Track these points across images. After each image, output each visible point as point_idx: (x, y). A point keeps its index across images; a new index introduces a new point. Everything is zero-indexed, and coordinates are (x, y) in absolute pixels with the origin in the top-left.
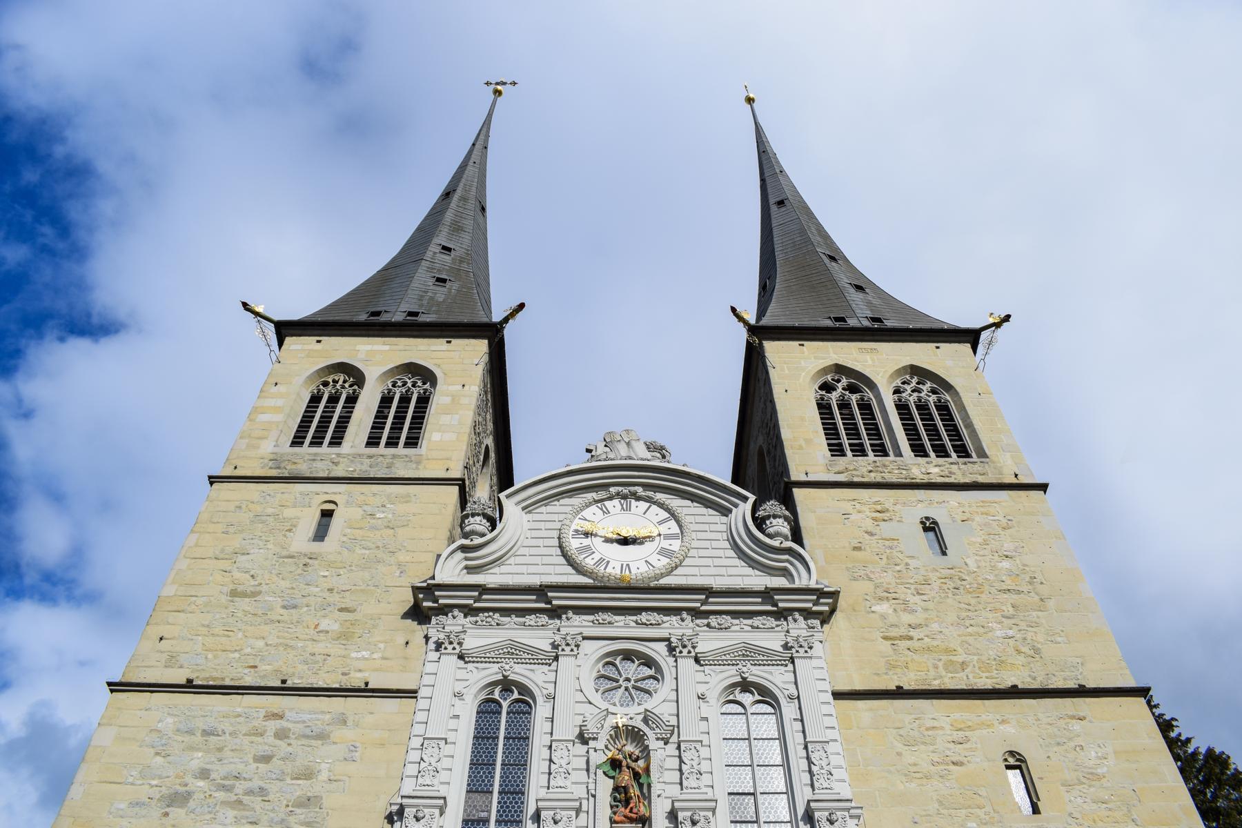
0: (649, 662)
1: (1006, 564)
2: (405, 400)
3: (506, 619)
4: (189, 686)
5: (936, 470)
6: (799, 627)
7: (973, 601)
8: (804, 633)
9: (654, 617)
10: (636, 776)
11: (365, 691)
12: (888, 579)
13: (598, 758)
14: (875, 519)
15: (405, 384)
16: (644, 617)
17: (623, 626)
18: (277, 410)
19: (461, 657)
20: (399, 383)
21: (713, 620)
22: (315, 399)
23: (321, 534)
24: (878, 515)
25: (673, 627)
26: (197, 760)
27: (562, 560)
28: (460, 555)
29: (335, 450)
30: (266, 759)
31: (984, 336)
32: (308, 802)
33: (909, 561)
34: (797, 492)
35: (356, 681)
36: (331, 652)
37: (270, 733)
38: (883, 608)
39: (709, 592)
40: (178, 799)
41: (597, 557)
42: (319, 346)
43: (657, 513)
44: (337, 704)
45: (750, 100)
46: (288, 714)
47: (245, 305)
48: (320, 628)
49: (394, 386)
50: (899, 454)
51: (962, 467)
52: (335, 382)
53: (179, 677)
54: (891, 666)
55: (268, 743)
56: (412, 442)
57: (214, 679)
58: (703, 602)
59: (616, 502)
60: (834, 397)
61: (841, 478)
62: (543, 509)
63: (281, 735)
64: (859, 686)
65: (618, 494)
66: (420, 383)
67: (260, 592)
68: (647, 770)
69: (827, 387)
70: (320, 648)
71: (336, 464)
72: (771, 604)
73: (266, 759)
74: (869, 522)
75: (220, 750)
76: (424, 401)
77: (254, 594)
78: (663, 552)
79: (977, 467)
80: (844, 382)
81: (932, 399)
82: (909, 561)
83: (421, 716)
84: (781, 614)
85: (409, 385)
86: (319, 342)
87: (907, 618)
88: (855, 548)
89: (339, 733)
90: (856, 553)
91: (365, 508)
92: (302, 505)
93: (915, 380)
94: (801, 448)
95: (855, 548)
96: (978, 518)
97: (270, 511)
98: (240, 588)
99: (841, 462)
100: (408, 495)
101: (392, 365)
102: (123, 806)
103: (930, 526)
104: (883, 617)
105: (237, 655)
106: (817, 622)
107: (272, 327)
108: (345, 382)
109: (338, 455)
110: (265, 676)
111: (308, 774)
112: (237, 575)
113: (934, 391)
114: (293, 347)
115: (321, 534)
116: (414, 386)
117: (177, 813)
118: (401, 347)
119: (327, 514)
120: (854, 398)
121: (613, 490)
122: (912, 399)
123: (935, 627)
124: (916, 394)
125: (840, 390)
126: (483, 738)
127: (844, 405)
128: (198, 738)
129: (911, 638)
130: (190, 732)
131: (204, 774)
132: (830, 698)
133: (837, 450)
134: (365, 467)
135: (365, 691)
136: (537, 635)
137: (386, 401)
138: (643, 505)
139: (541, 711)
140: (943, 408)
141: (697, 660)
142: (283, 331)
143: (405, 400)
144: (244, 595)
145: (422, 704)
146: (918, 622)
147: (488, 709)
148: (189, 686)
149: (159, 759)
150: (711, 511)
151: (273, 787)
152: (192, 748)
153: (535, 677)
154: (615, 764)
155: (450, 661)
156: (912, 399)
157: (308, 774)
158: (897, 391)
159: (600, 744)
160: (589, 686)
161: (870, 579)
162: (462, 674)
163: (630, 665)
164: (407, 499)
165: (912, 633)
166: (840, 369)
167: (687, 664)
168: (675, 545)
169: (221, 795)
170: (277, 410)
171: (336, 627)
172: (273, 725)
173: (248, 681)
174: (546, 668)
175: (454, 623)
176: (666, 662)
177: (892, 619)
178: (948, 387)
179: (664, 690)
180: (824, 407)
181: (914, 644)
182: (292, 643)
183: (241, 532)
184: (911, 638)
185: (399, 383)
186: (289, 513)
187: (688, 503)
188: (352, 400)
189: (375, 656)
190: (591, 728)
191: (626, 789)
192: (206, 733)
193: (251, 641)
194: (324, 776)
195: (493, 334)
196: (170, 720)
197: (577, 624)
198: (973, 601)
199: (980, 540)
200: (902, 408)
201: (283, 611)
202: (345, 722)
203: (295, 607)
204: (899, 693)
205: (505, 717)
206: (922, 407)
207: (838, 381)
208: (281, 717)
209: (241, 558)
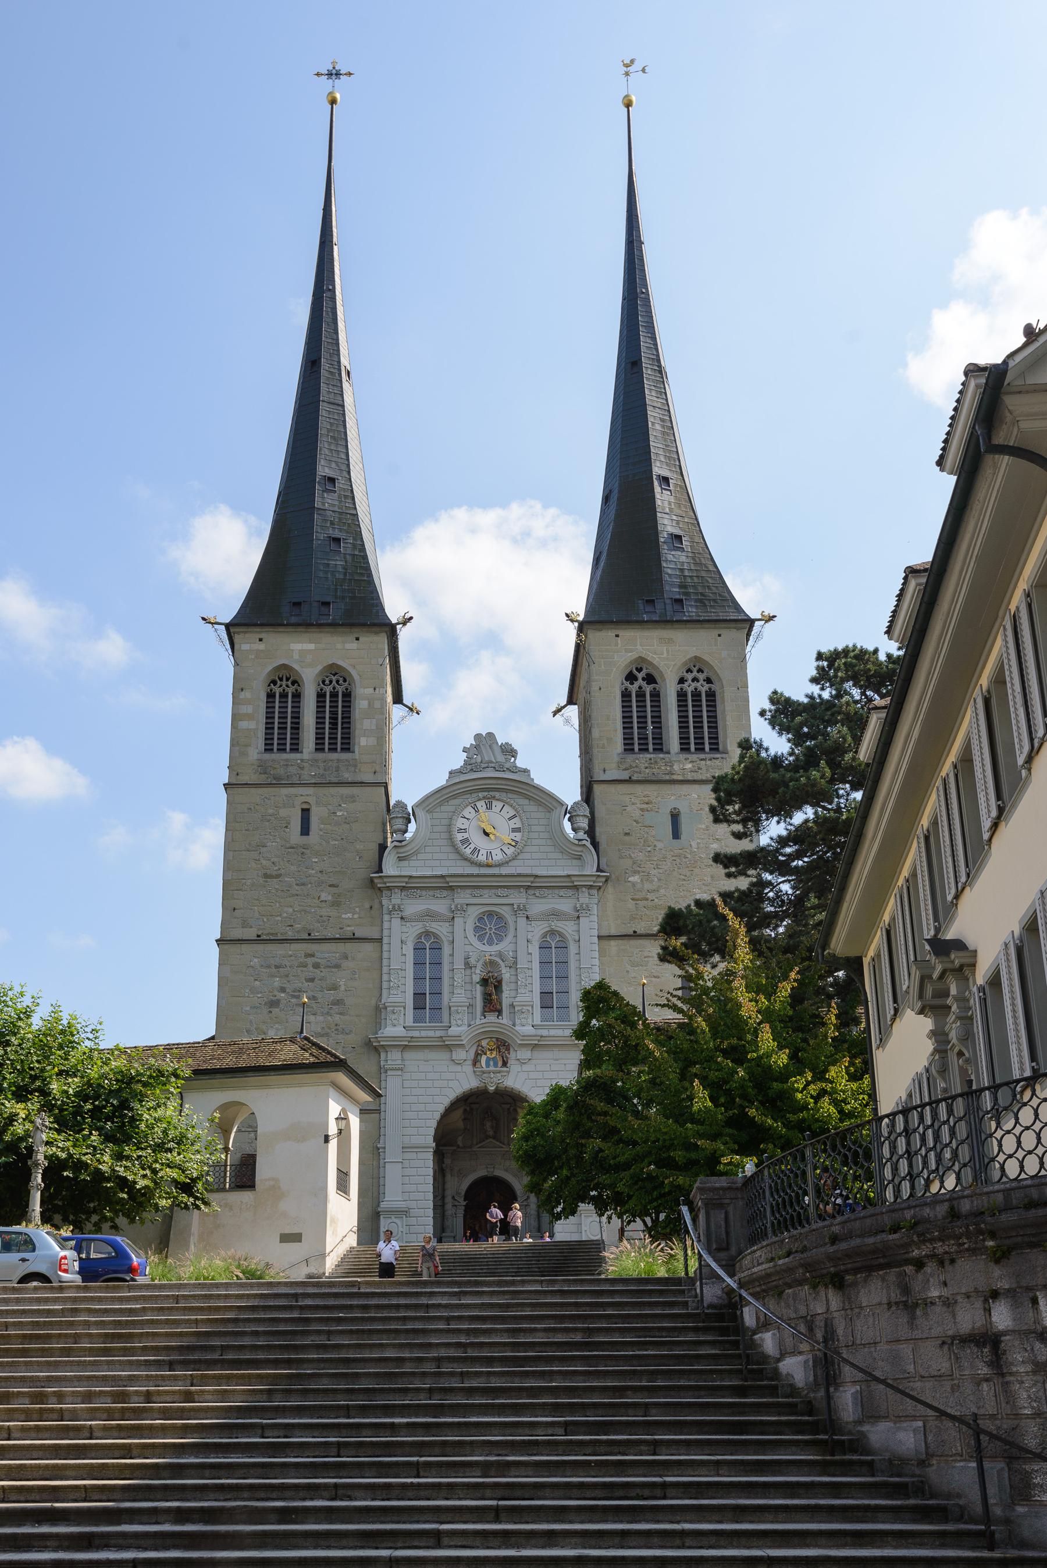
0: (500, 917)
2: (334, 695)
3: (424, 893)
4: (259, 940)
6: (584, 898)
7: (688, 874)
8: (587, 900)
9: (505, 892)
10: (496, 987)
11: (353, 938)
12: (640, 856)
13: (477, 978)
14: (642, 810)
15: (331, 682)
16: (499, 892)
17: (488, 898)
18: (249, 717)
19: (402, 918)
20: (327, 682)
21: (537, 893)
22: (270, 696)
23: (305, 830)
24: (645, 806)
25: (517, 898)
26: (277, 982)
27: (450, 849)
28: (394, 852)
29: (298, 756)
30: (312, 980)
31: (757, 623)
32: (338, 1002)
33: (656, 843)
34: (597, 789)
35: (348, 930)
36: (331, 914)
37: (310, 966)
38: (635, 879)
39: (537, 876)
40: (274, 1004)
41: (472, 846)
42: (261, 646)
43: (509, 811)
44: (341, 947)
45: (628, 105)
46: (317, 954)
47: (204, 619)
48: (322, 898)
49: (323, 682)
50: (668, 753)
51: (708, 762)
52: (281, 679)
53: (251, 933)
54: (633, 918)
55: (310, 971)
56: (347, 748)
57: (272, 934)
58: (532, 885)
59: (482, 803)
60: (634, 688)
61: (625, 776)
62: (438, 810)
63: (316, 966)
64: (613, 932)
67: (280, 875)
68: (500, 982)
69: (631, 677)
70: (324, 912)
71: (302, 768)
72: (571, 885)
73: (312, 980)
74: (638, 812)
75: (287, 976)
76: (348, 695)
77: (278, 876)
79: (717, 762)
80: (644, 671)
81: (703, 688)
82: (656, 843)
83: (385, 955)
84: (576, 888)
85: (334, 682)
86: (261, 640)
87: (647, 886)
88: (627, 834)
89: (345, 964)
90: (627, 838)
91: (330, 807)
92: (286, 804)
93: (695, 670)
94: (603, 747)
95: (627, 834)
97: (270, 811)
98: (268, 872)
99: (630, 758)
100: (353, 796)
101: (320, 668)
102: (248, 1009)
103: (675, 817)
104: (634, 884)
105: (279, 918)
106: (594, 892)
107: (223, 627)
108: (288, 679)
109: (302, 760)
110: (298, 932)
111: (335, 987)
112: (264, 862)
113: (709, 681)
114: (245, 647)
115: (305, 830)
116: (337, 682)
117: (276, 1011)
119: (306, 813)
120: (648, 689)
121: (481, 795)
122: (689, 690)
123: (662, 891)
125: (640, 681)
126: (418, 964)
127: (641, 695)
128: (274, 970)
129: (647, 899)
130: (269, 967)
131: (283, 990)
132: (596, 940)
133: (628, 748)
134: (321, 771)
135: (353, 938)
136: (440, 905)
137: (321, 696)
138: (500, 805)
139: (446, 950)
140: (711, 695)
141: (527, 918)
142: (232, 630)
144: (271, 877)
145: (385, 947)
146: (654, 888)
147: (418, 949)
148: (259, 940)
149: (257, 983)
150: (541, 809)
151: (319, 995)
152: (272, 976)
153: (441, 929)
154: (485, 982)
155: (396, 922)
156: (689, 690)
157: (335, 987)
158: (682, 681)
159: (478, 971)
160: (470, 933)
161: (631, 857)
162: (405, 929)
163: (491, 924)
164: (353, 798)
165: (650, 896)
166: (640, 664)
167: (522, 921)
168: (518, 836)
169: (294, 1000)
171: (330, 898)
172: (310, 961)
173: (290, 934)
174: (447, 924)
175: (397, 899)
176: (510, 919)
177: (639, 886)
178: (720, 679)
179: (510, 937)
180: (626, 695)
181: (650, 903)
182: (308, 909)
183: (257, 829)
184: (647, 899)
185: (327, 682)
186: (283, 812)
187: (526, 802)
188: (297, 696)
189: (356, 916)
190: (472, 961)
191: (490, 995)
192: (276, 967)
193: (286, 909)
194: (343, 988)
195: (391, 631)
196: (256, 960)
197: (463, 898)
198: (688, 874)
199: (703, 826)
200: (681, 696)
201: (297, 888)
202: (347, 958)
203: (303, 884)
204: (635, 935)
205: (429, 953)
206: (696, 694)
207: (639, 670)
208: (313, 956)
209: (263, 850)
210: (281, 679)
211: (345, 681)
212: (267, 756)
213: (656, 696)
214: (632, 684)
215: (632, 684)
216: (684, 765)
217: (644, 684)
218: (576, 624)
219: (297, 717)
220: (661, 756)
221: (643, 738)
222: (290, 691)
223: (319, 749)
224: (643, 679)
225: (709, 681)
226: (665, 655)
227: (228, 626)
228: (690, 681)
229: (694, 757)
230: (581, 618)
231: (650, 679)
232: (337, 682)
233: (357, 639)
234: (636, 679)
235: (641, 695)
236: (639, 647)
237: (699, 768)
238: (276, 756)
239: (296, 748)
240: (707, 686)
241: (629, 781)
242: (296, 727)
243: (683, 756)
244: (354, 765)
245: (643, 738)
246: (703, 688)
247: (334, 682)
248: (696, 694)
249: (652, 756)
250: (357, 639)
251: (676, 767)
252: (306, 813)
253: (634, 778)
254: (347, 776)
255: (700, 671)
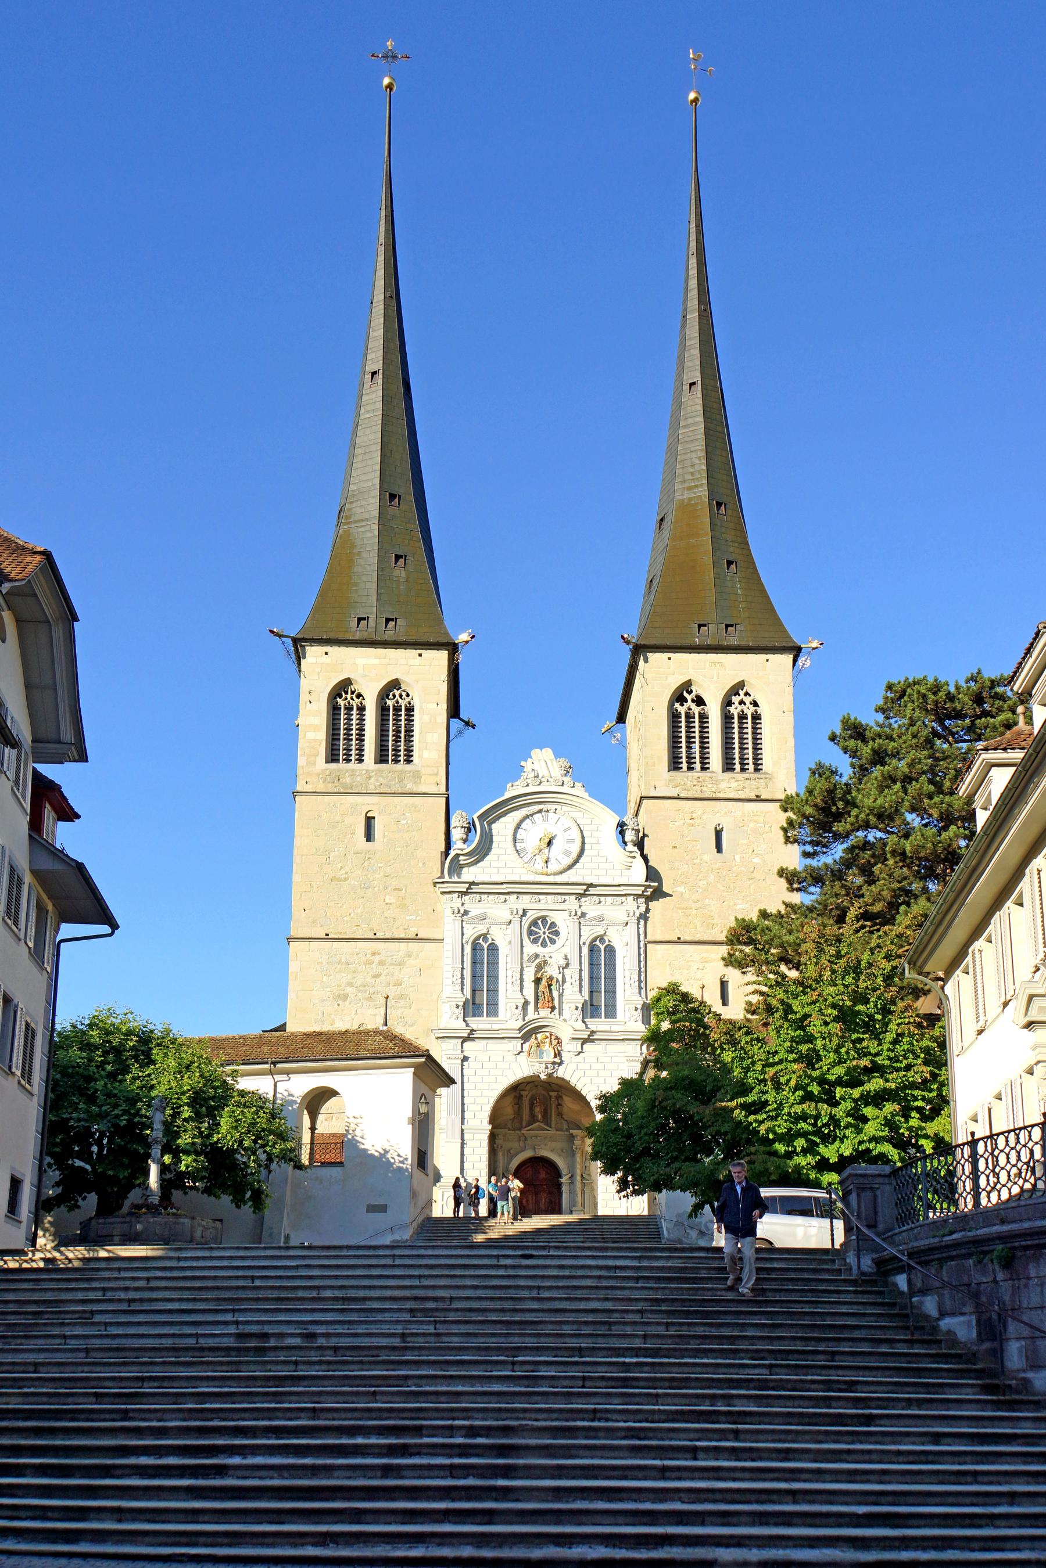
1: (756, 860)
2: (398, 709)
5: (734, 785)
9: (560, 898)
15: (394, 696)
18: (315, 728)
23: (369, 836)
52: (346, 693)
65: (540, 811)
66: (404, 694)
69: (679, 697)
76: (410, 710)
78: (567, 853)
81: (749, 710)
85: (397, 697)
96: (751, 825)
97: (338, 818)
115: (369, 836)
116: (401, 696)
118: (386, 661)
119: (369, 821)
120: (696, 710)
121: (537, 808)
124: (740, 707)
127: (689, 717)
133: (674, 765)
140: (756, 717)
143: (398, 709)
170: (315, 728)
180: (674, 717)
186: (348, 820)
188: (362, 709)
200: (727, 718)
206: (742, 717)
210: (346, 693)
211: (408, 695)
212: (334, 765)
213: (703, 717)
214: (682, 705)
215: (682, 705)
216: (732, 784)
217: (693, 706)
218: (631, 646)
219: (361, 730)
220: (709, 775)
221: (690, 758)
222: (355, 703)
223: (382, 758)
224: (693, 701)
225: (755, 704)
226: (715, 678)
227: (296, 641)
228: (737, 703)
229: (741, 776)
230: (634, 641)
231: (700, 701)
232: (401, 696)
233: (420, 655)
234: (686, 701)
235: (689, 717)
236: (691, 671)
237: (744, 787)
238: (341, 765)
239: (360, 760)
240: (752, 709)
241: (678, 798)
242: (361, 739)
243: (728, 775)
244: (417, 776)
245: (690, 758)
246: (749, 710)
247: (397, 697)
248: (742, 717)
249: (700, 774)
250: (420, 655)
251: (723, 785)
252: (369, 821)
253: (682, 795)
254: (410, 787)
255: (747, 694)
